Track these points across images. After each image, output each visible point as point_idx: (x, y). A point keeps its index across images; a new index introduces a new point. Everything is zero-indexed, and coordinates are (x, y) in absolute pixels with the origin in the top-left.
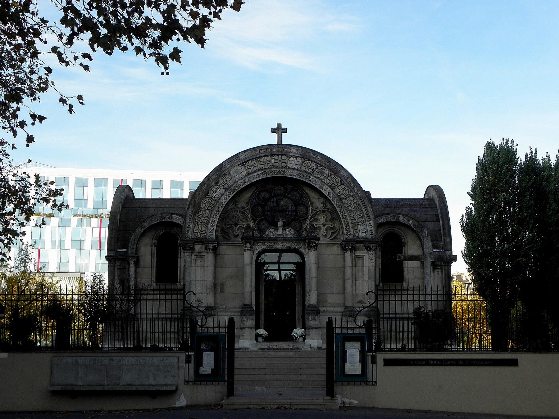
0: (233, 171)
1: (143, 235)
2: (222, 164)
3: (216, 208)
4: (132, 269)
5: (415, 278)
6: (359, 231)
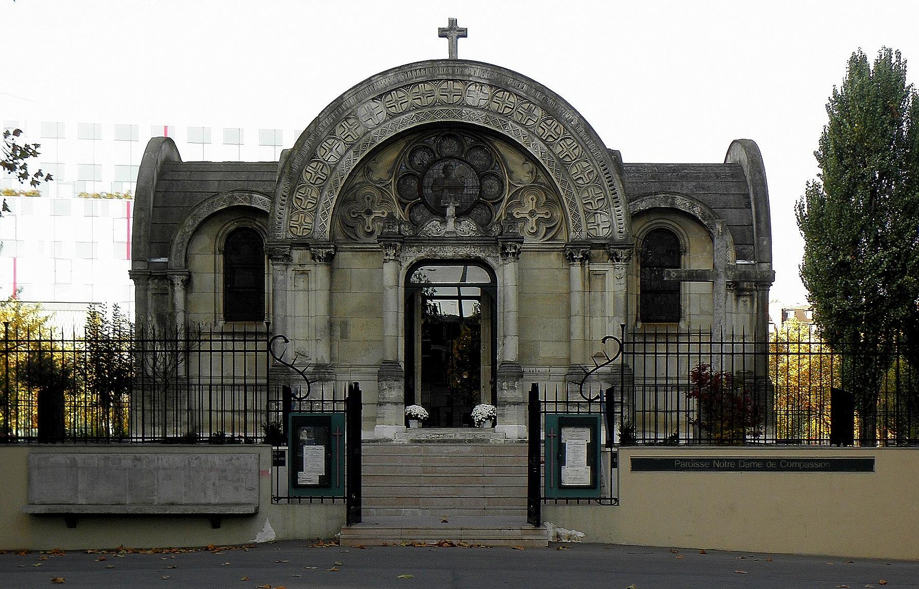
0: (362, 111)
1: (197, 231)
2: (341, 97)
3: (331, 181)
4: (179, 295)
5: (702, 313)
6: (598, 225)
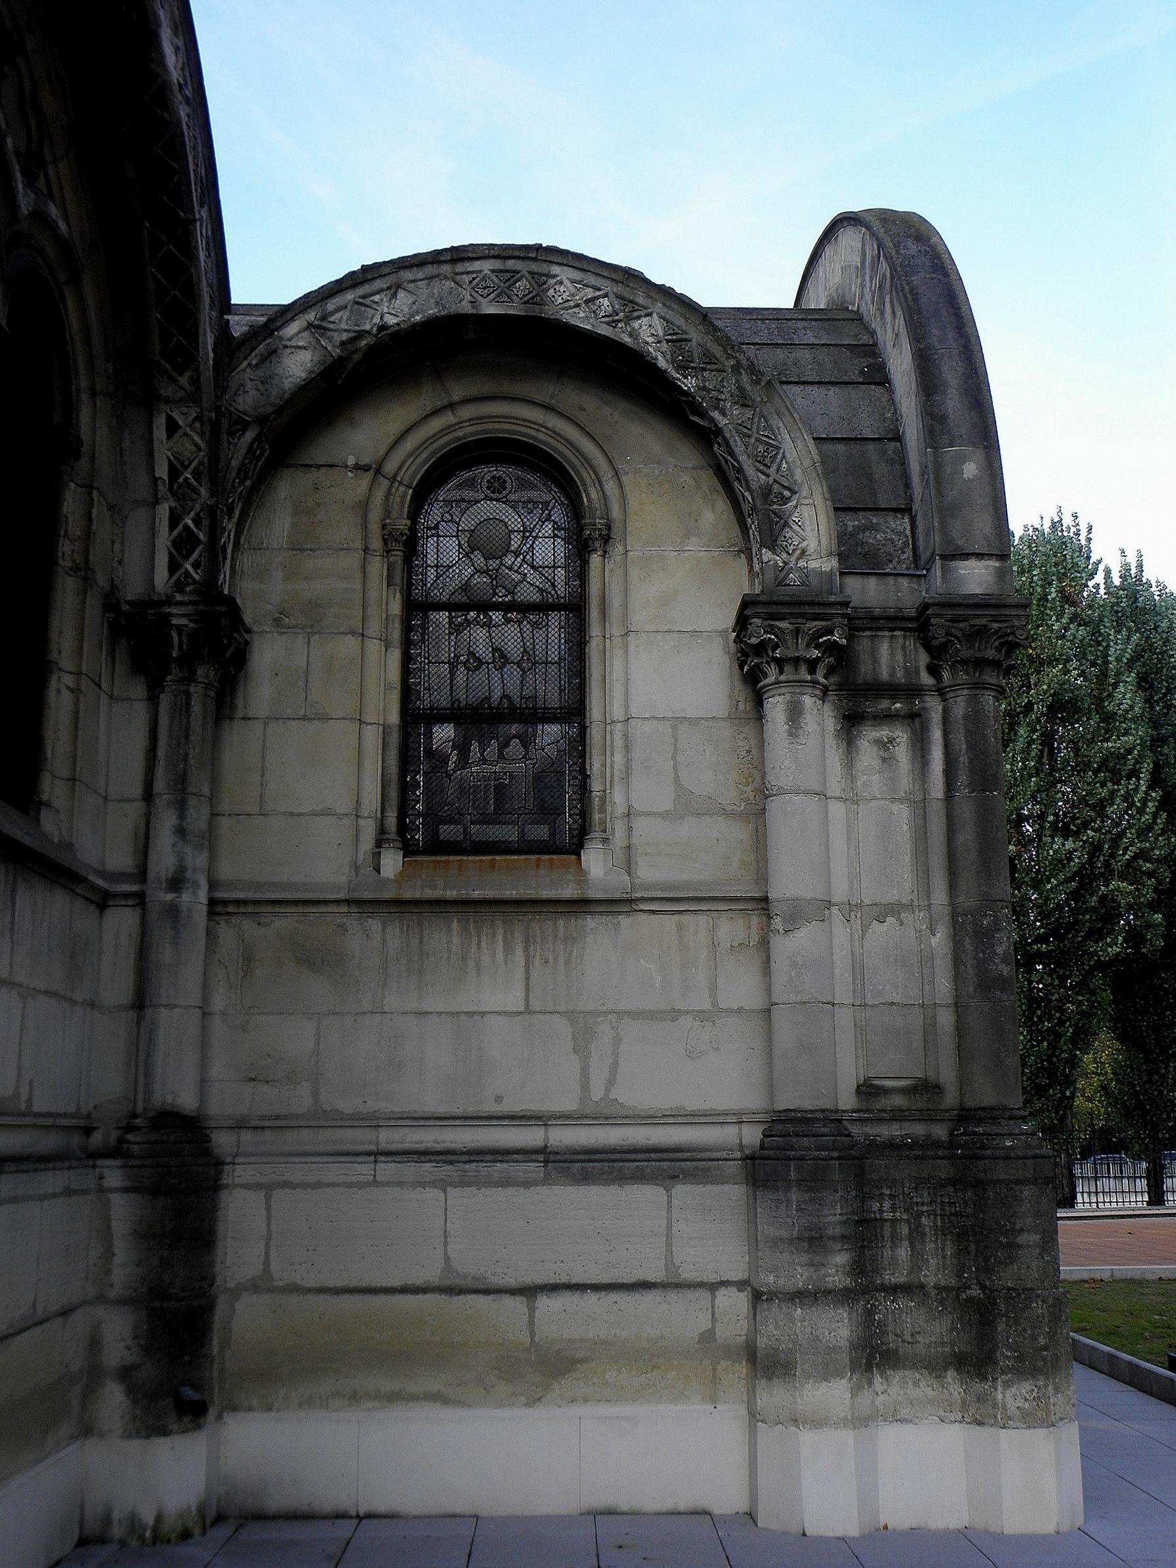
5: (687, 805)
